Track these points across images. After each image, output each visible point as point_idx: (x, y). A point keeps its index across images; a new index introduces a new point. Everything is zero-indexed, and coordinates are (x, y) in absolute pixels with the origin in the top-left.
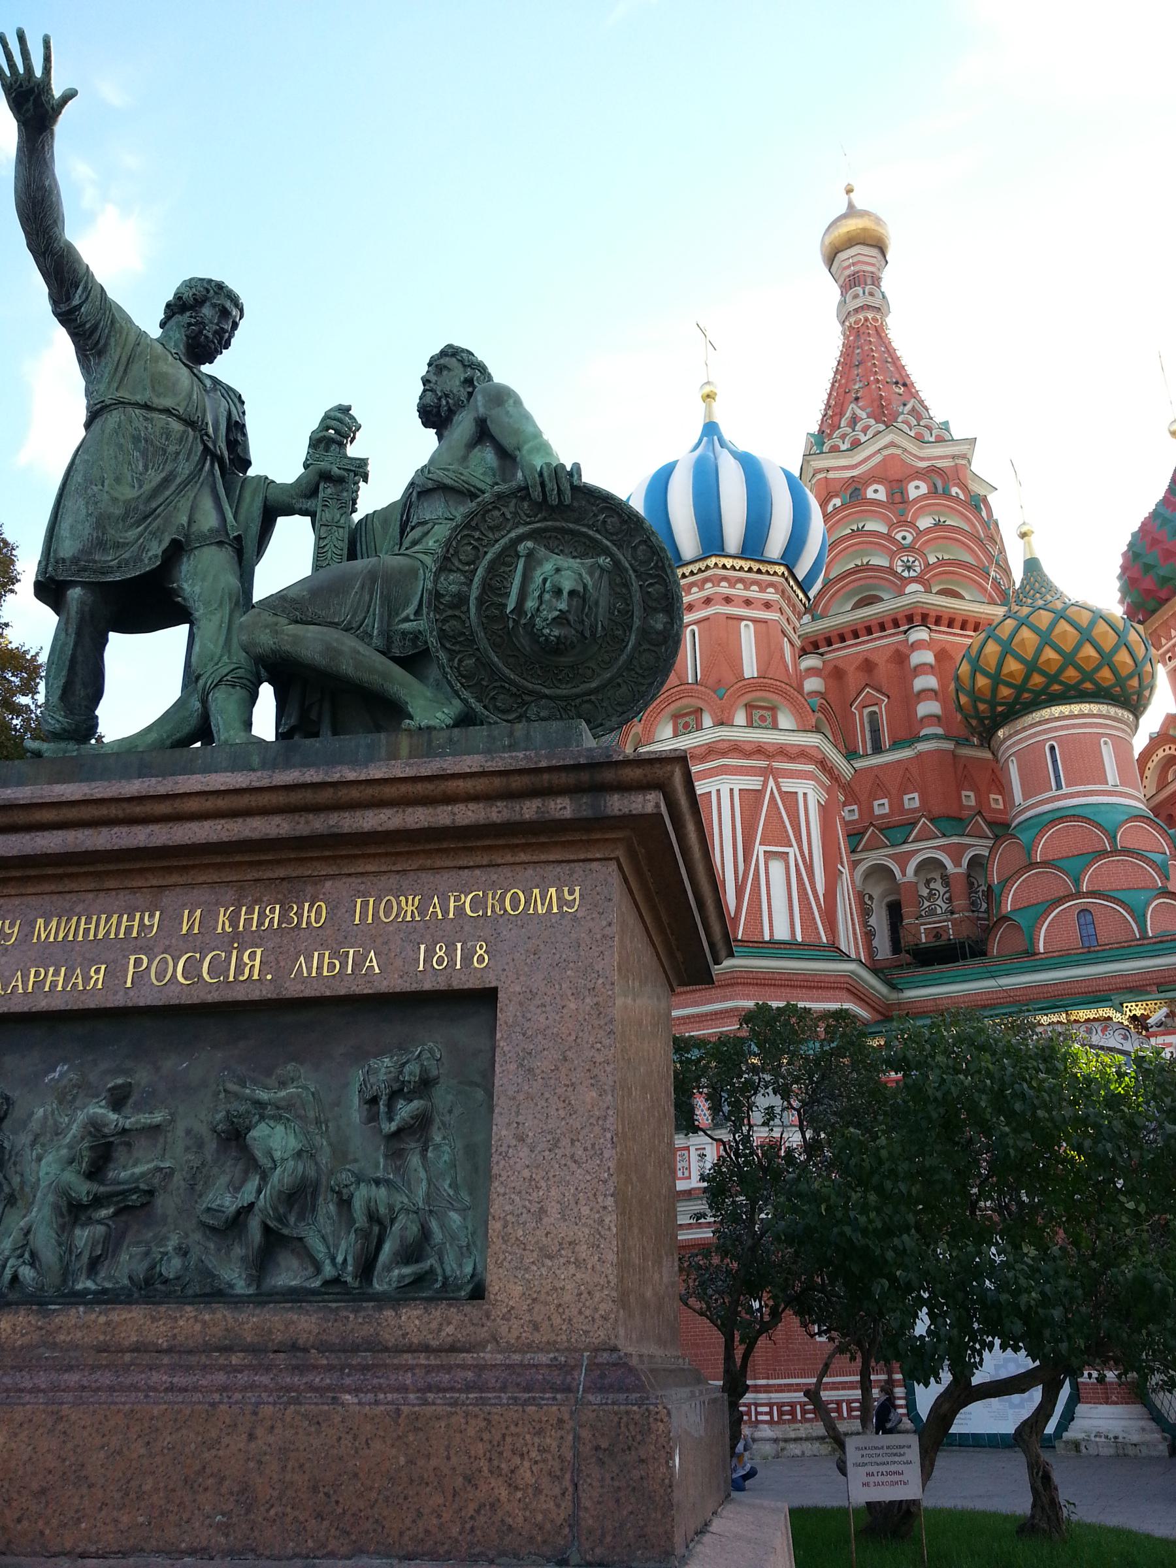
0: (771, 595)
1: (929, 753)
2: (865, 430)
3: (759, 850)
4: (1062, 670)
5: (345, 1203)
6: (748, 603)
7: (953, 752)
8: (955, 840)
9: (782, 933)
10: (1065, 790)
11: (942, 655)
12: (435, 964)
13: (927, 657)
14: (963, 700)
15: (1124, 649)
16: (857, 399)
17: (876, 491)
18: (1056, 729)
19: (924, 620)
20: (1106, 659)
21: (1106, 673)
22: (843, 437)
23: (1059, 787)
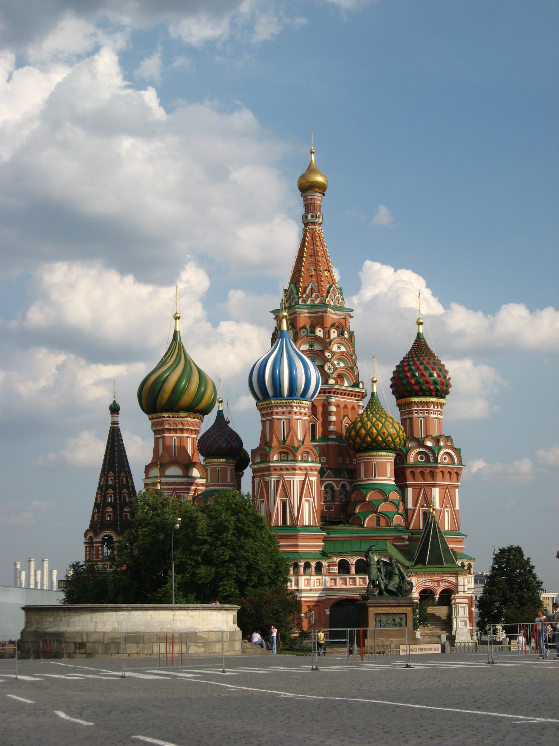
0: (307, 411)
1: (332, 445)
2: (317, 296)
3: (304, 499)
4: (381, 443)
5: (400, 624)
6: (301, 414)
7: (338, 445)
8: (338, 479)
9: (307, 524)
10: (376, 478)
11: (338, 406)
12: (404, 612)
13: (333, 409)
14: (351, 441)
15: (398, 438)
16: (311, 276)
17: (320, 331)
18: (377, 459)
19: (334, 393)
20: (393, 440)
21: (392, 444)
22: (308, 297)
23: (375, 477)
